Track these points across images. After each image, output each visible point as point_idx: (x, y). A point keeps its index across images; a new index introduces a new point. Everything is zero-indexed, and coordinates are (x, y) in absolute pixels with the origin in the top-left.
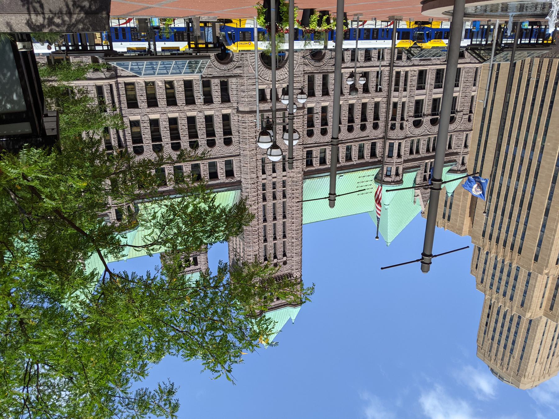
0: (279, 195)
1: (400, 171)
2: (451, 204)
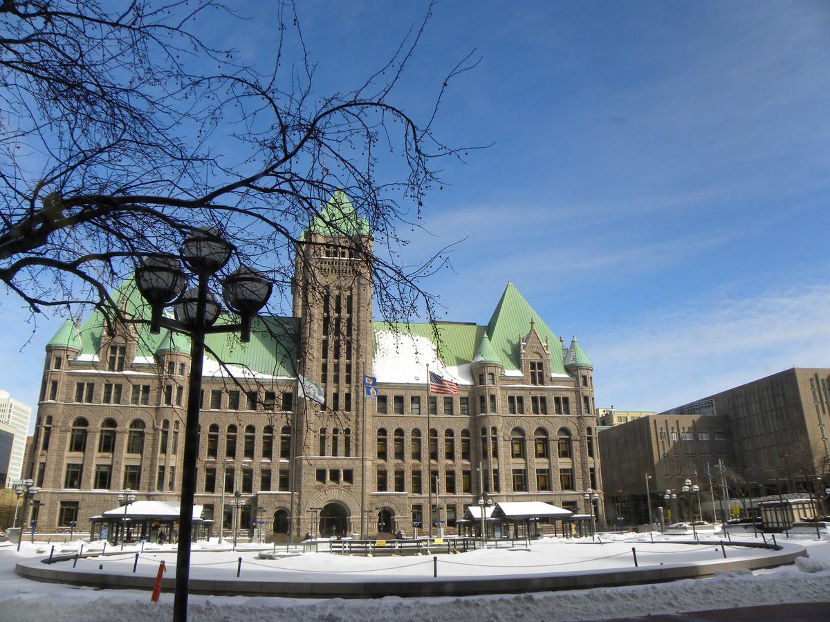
0: (331, 368)
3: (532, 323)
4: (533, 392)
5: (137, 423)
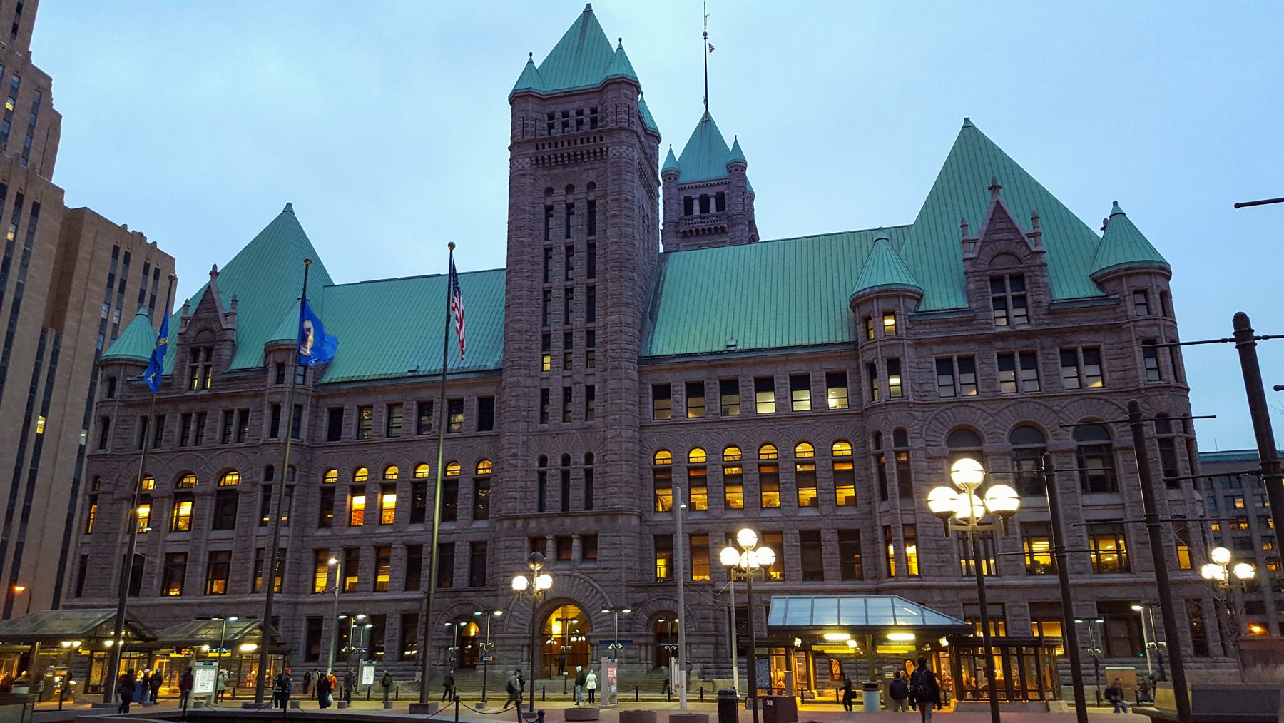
1: (272, 375)
2: (110, 285)
3: (995, 188)
4: (999, 344)
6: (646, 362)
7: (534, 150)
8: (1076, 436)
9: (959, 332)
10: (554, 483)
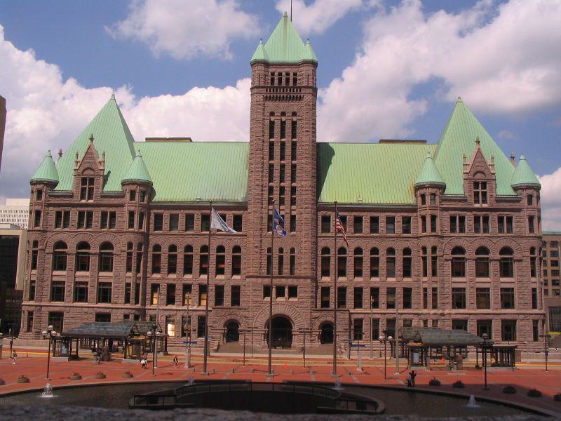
1: (128, 196)
5: (107, 245)
6: (319, 207)
7: (265, 92)
8: (501, 254)
9: (460, 205)
10: (275, 262)
